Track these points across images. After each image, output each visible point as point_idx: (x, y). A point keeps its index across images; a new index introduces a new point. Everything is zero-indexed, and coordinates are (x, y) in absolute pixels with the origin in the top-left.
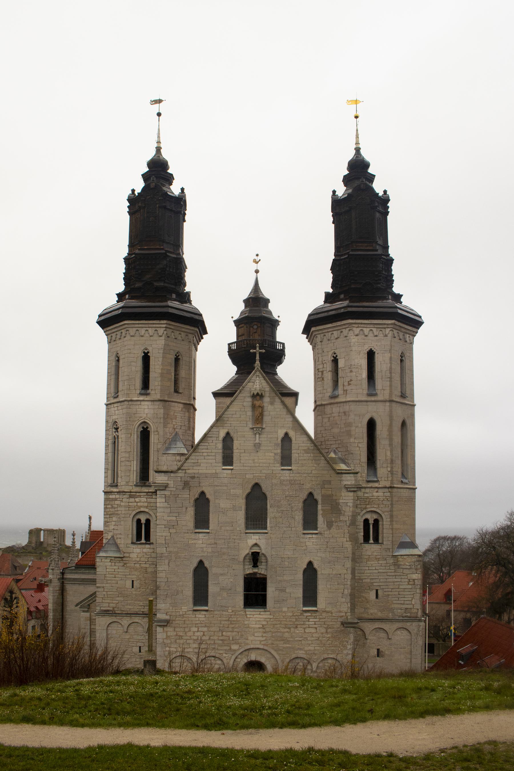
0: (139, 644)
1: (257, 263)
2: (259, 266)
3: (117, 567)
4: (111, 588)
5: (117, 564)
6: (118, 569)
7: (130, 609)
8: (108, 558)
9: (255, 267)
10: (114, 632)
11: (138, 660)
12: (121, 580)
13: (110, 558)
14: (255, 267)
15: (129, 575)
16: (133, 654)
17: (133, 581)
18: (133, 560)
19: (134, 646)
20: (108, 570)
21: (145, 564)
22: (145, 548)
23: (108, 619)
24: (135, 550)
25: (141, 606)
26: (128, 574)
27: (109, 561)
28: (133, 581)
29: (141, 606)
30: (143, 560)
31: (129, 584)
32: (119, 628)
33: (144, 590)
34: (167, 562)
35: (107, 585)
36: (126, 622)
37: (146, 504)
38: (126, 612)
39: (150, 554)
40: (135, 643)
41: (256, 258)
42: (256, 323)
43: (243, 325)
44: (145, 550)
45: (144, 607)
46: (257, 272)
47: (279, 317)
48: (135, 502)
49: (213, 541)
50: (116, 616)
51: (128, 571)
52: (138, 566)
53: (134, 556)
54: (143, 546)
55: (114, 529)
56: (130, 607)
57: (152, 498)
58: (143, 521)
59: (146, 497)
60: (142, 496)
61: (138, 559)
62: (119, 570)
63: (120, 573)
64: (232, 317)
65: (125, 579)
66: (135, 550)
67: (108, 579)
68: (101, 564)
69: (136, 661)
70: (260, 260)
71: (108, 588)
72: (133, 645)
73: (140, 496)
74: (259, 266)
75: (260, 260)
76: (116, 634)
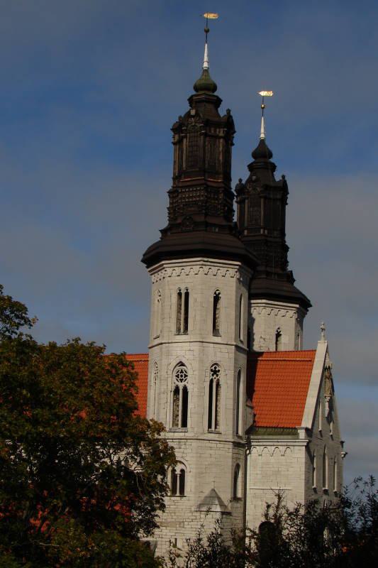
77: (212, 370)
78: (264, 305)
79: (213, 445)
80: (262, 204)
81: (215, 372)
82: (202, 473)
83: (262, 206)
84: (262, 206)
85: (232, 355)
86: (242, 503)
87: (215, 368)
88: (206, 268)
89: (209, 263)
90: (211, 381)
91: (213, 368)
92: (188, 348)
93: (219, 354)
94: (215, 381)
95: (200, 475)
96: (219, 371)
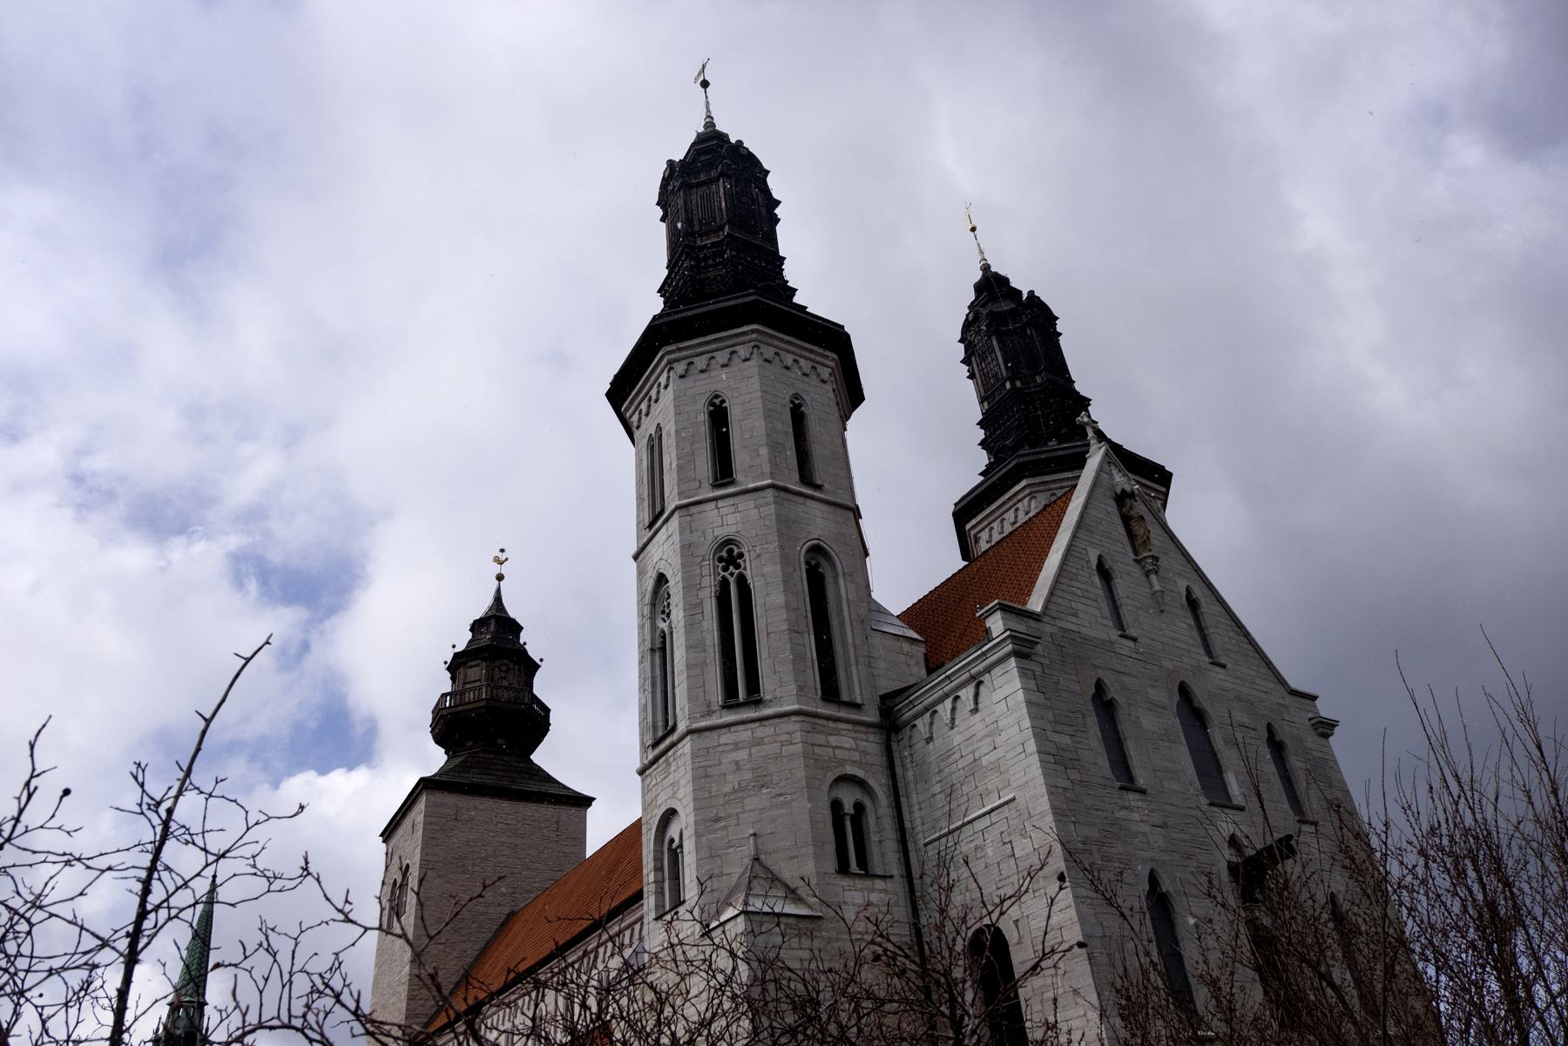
1: (501, 563)
2: (505, 569)
9: (496, 569)
14: (496, 569)
22: (873, 890)
41: (500, 555)
42: (505, 661)
46: (500, 578)
48: (828, 745)
49: (1157, 818)
55: (755, 835)
57: (867, 741)
58: (848, 808)
59: (852, 734)
64: (454, 646)
70: (507, 559)
73: (837, 733)
74: (505, 569)
75: (507, 559)
77: (721, 560)
78: (1028, 491)
79: (744, 734)
80: (995, 343)
82: (717, 820)
83: (997, 350)
84: (997, 350)
85: (771, 510)
86: (897, 887)
87: (730, 552)
88: (680, 367)
89: (684, 353)
90: (724, 584)
91: (724, 554)
92: (664, 538)
93: (731, 519)
95: (708, 823)
96: (741, 555)
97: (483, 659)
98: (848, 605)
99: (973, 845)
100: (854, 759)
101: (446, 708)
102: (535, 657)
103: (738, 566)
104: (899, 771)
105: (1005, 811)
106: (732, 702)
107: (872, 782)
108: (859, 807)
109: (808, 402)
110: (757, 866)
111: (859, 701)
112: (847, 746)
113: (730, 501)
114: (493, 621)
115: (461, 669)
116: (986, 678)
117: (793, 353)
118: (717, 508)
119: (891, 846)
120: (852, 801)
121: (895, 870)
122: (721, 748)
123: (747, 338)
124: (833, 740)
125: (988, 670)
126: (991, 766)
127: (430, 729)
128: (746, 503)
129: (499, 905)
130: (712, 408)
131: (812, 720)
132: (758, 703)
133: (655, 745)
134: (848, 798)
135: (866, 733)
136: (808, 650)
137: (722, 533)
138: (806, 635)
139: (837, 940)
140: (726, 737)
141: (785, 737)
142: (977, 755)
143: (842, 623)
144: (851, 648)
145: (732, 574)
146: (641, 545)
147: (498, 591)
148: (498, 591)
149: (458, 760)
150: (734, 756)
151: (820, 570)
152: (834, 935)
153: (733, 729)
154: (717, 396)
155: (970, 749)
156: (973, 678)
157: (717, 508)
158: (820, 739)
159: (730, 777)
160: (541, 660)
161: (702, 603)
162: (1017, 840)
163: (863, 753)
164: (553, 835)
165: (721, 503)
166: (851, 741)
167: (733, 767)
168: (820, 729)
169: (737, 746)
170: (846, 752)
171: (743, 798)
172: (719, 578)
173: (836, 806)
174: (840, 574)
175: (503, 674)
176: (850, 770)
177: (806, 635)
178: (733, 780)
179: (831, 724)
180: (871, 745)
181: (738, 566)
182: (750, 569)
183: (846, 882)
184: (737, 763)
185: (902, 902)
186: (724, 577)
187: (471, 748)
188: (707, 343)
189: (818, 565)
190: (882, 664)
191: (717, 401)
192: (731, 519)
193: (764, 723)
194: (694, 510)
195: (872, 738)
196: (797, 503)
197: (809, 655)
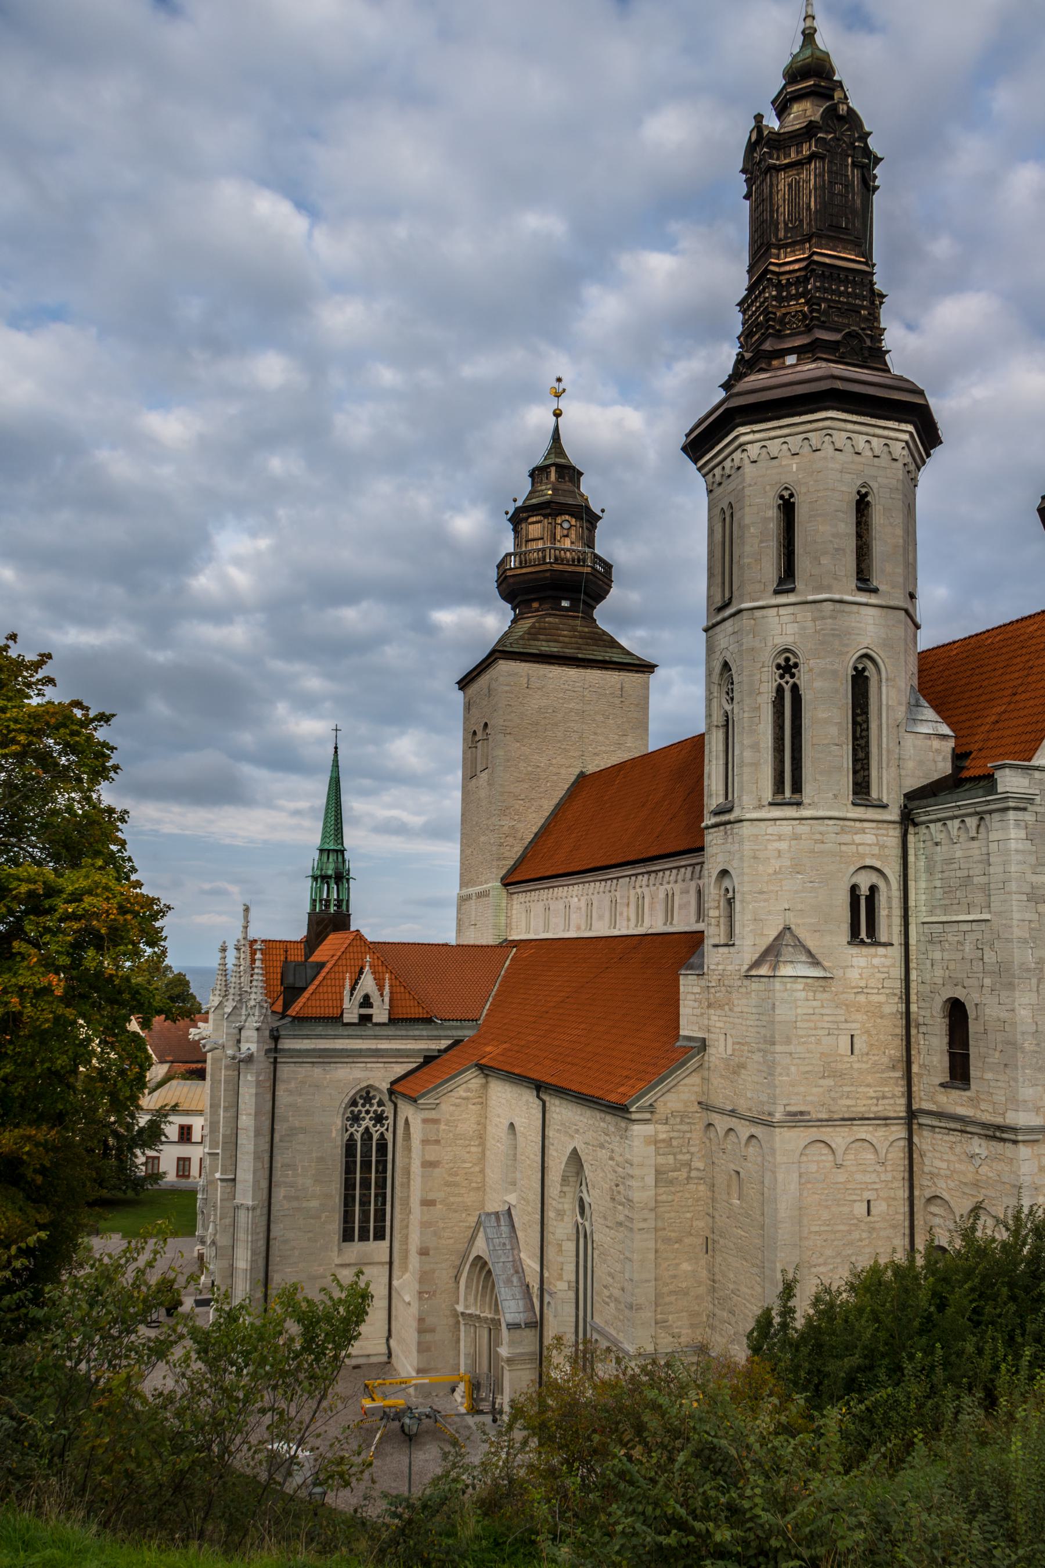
0: (867, 1195)
1: (558, 395)
3: (815, 1003)
4: (807, 1055)
5: (819, 996)
6: (823, 1007)
7: (849, 1106)
8: (800, 980)
10: (813, 1168)
11: (864, 1235)
12: (829, 1034)
13: (804, 980)
15: (846, 1021)
16: (855, 1221)
17: (852, 1036)
18: (853, 984)
19: (855, 1201)
20: (799, 1011)
21: (878, 994)
22: (876, 956)
23: (802, 1135)
24: (855, 961)
25: (872, 1098)
26: (843, 1019)
27: (800, 987)
28: (852, 1036)
29: (872, 1098)
30: (873, 985)
31: (844, 1042)
32: (823, 1158)
33: (877, 1058)
34: (1034, 981)
35: (800, 1049)
36: (839, 1140)
37: (876, 850)
38: (841, 1116)
39: (886, 970)
40: (859, 1192)
41: (556, 385)
42: (567, 517)
43: (538, 518)
44: (876, 961)
45: (878, 1099)
46: (557, 414)
47: (603, 511)
50: (886, 1125)
51: (842, 1012)
52: (862, 998)
53: (853, 974)
54: (865, 950)
56: (849, 1102)
57: (887, 836)
59: (873, 832)
60: (867, 831)
61: (863, 984)
62: (824, 1011)
63: (826, 1018)
64: (515, 500)
65: (836, 1032)
66: (855, 961)
67: (801, 1032)
68: (785, 995)
69: (861, 1240)
70: (564, 390)
71: (802, 1056)
72: (855, 1197)
73: (863, 831)
75: (564, 390)
76: (817, 1171)
79: (786, 828)
81: (787, 668)
86: (896, 953)
87: (787, 659)
89: (758, 436)
90: (780, 690)
92: (730, 630)
93: (792, 628)
94: (787, 688)
96: (796, 665)
97: (545, 516)
98: (887, 710)
99: (956, 939)
100: (873, 852)
101: (511, 569)
102: (596, 509)
103: (793, 676)
104: (911, 859)
105: (983, 926)
106: (779, 798)
107: (886, 871)
108: (873, 889)
109: (875, 491)
110: (788, 935)
111: (885, 801)
112: (869, 842)
113: (790, 610)
114: (553, 469)
115: (524, 525)
116: (987, 817)
117: (867, 434)
118: (778, 615)
119: (897, 920)
120: (868, 885)
121: (897, 939)
122: (767, 837)
123: (821, 424)
124: (858, 838)
125: (990, 812)
126: (979, 886)
127: (496, 585)
128: (805, 614)
129: (569, 767)
130: (781, 502)
131: (841, 823)
132: (799, 804)
133: (720, 609)
134: (865, 881)
135: (887, 829)
136: (845, 761)
137: (781, 641)
138: (845, 747)
139: (843, 993)
140: (772, 829)
141: (818, 837)
142: (971, 873)
143: (880, 726)
144: (884, 752)
145: (787, 683)
146: (710, 624)
147: (556, 429)
148: (556, 429)
149: (526, 624)
150: (776, 845)
151: (866, 674)
152: (841, 989)
153: (778, 822)
154: (786, 489)
155: (967, 866)
156: (977, 813)
157: (778, 615)
158: (846, 838)
159: (773, 861)
160: (603, 511)
161: (759, 707)
162: (987, 949)
163: (883, 847)
164: (617, 701)
165: (783, 611)
166: (874, 837)
167: (776, 854)
168: (848, 829)
169: (780, 838)
170: (867, 848)
171: (781, 880)
172: (775, 684)
173: (854, 889)
174: (884, 680)
175: (565, 532)
176: (868, 862)
177: (845, 747)
178: (775, 864)
179: (858, 824)
180: (892, 837)
181: (793, 676)
182: (803, 678)
183: (854, 950)
184: (779, 851)
185: (898, 964)
186: (780, 685)
187: (537, 610)
188: (780, 427)
189: (864, 669)
190: (910, 765)
191: (786, 494)
192: (792, 628)
193: (804, 822)
194: (758, 614)
195: (892, 833)
196: (850, 613)
197: (845, 766)
